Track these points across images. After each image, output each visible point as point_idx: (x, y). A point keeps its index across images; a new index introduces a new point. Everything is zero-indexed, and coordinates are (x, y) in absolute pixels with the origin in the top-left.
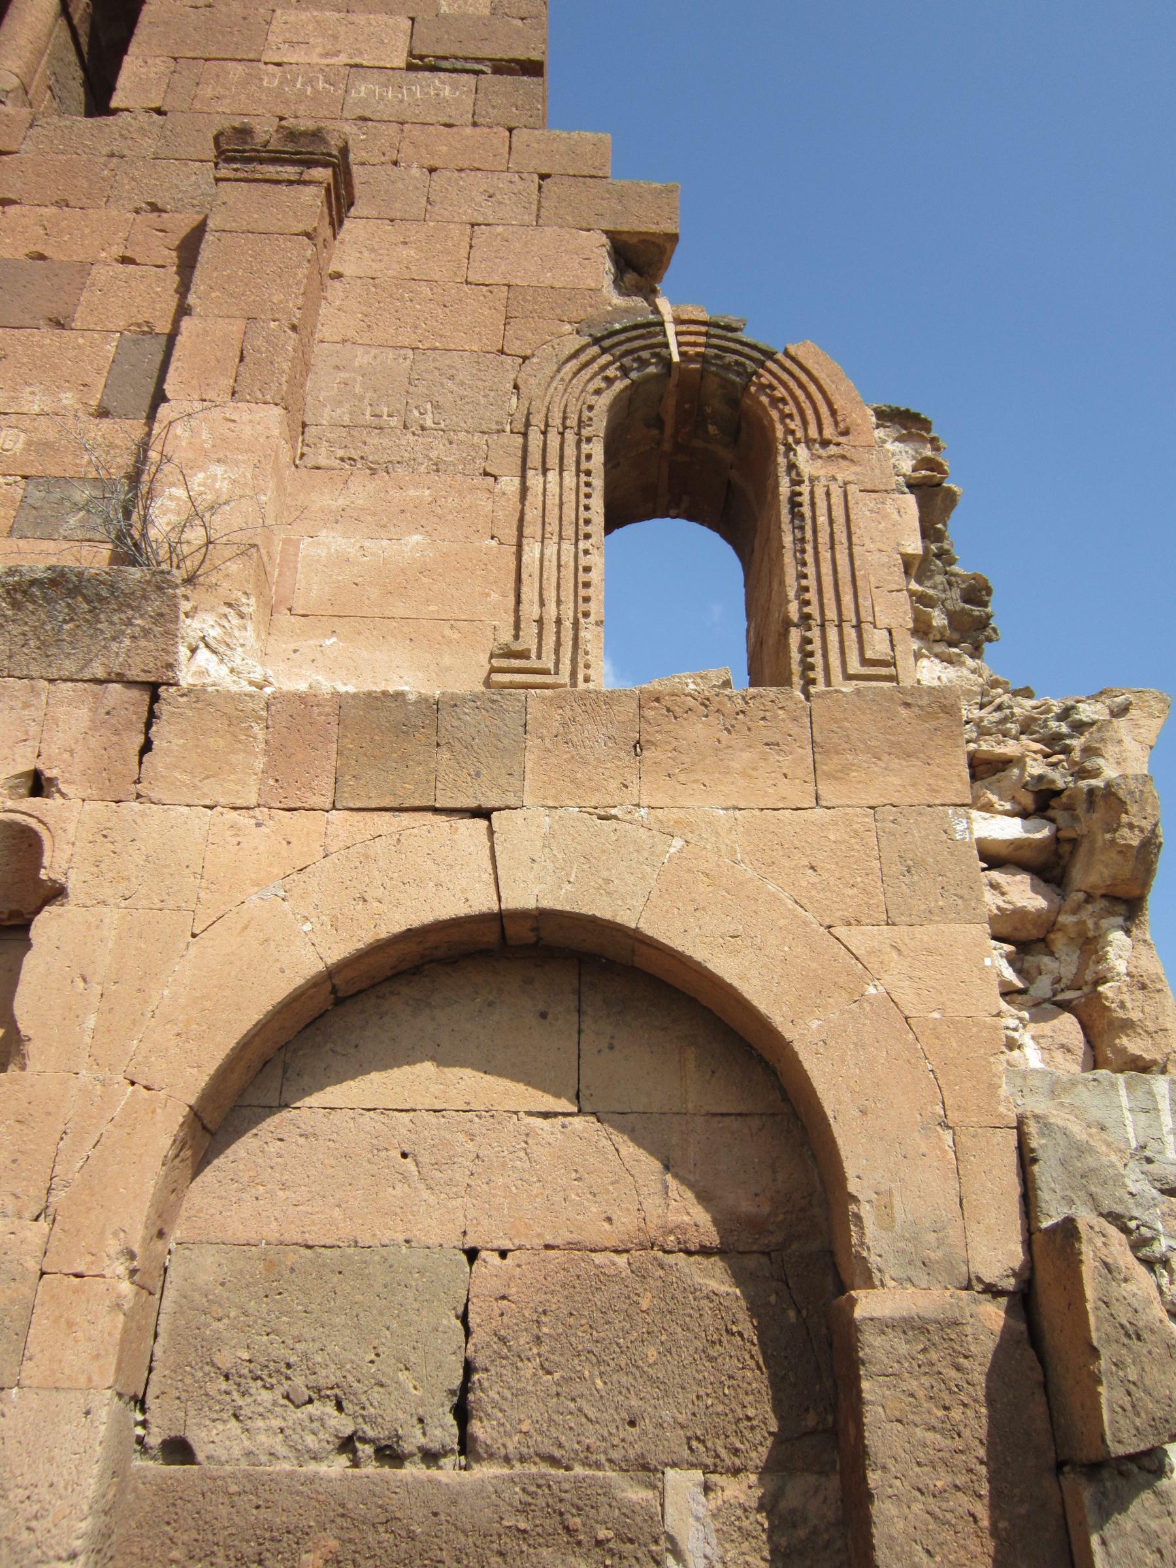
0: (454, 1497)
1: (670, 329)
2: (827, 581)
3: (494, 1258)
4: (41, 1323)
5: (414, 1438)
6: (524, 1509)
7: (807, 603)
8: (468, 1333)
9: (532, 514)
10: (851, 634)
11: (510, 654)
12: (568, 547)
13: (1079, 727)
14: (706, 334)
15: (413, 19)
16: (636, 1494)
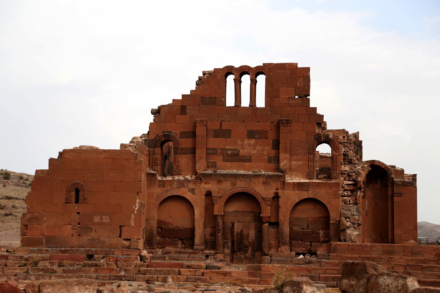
0: (308, 231)
1: (322, 137)
2: (334, 166)
3: (309, 218)
4: (285, 222)
5: (305, 228)
6: (311, 232)
7: (332, 168)
8: (308, 222)
9: (310, 160)
10: (336, 171)
11: (308, 174)
12: (313, 163)
13: (359, 173)
14: (325, 137)
15: (295, 88)
16: (318, 231)
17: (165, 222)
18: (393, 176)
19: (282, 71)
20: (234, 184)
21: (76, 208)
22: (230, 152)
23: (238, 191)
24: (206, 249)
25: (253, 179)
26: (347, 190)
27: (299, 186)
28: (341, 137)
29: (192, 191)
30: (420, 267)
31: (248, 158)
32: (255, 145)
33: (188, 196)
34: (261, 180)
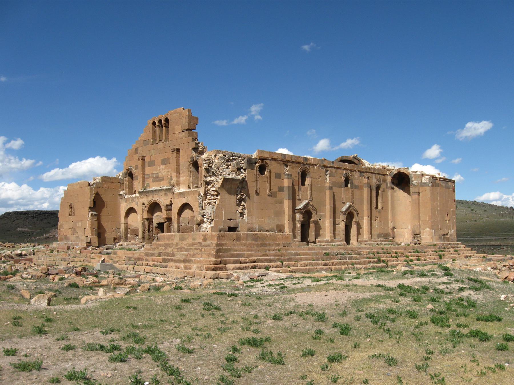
17: (131, 225)
18: (413, 179)
19: (176, 115)
20: (153, 197)
21: (72, 218)
22: (154, 176)
23: (152, 202)
24: (143, 242)
25: (160, 193)
26: (213, 195)
27: (182, 195)
28: (213, 156)
29: (137, 204)
30: (184, 249)
31: (162, 178)
32: (165, 169)
33: (136, 207)
34: (163, 193)
